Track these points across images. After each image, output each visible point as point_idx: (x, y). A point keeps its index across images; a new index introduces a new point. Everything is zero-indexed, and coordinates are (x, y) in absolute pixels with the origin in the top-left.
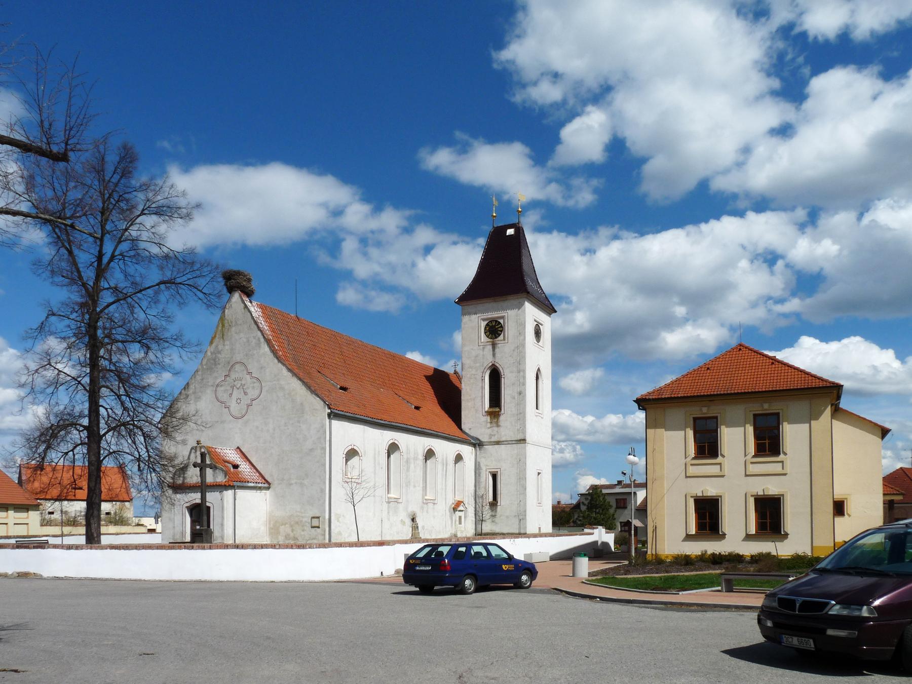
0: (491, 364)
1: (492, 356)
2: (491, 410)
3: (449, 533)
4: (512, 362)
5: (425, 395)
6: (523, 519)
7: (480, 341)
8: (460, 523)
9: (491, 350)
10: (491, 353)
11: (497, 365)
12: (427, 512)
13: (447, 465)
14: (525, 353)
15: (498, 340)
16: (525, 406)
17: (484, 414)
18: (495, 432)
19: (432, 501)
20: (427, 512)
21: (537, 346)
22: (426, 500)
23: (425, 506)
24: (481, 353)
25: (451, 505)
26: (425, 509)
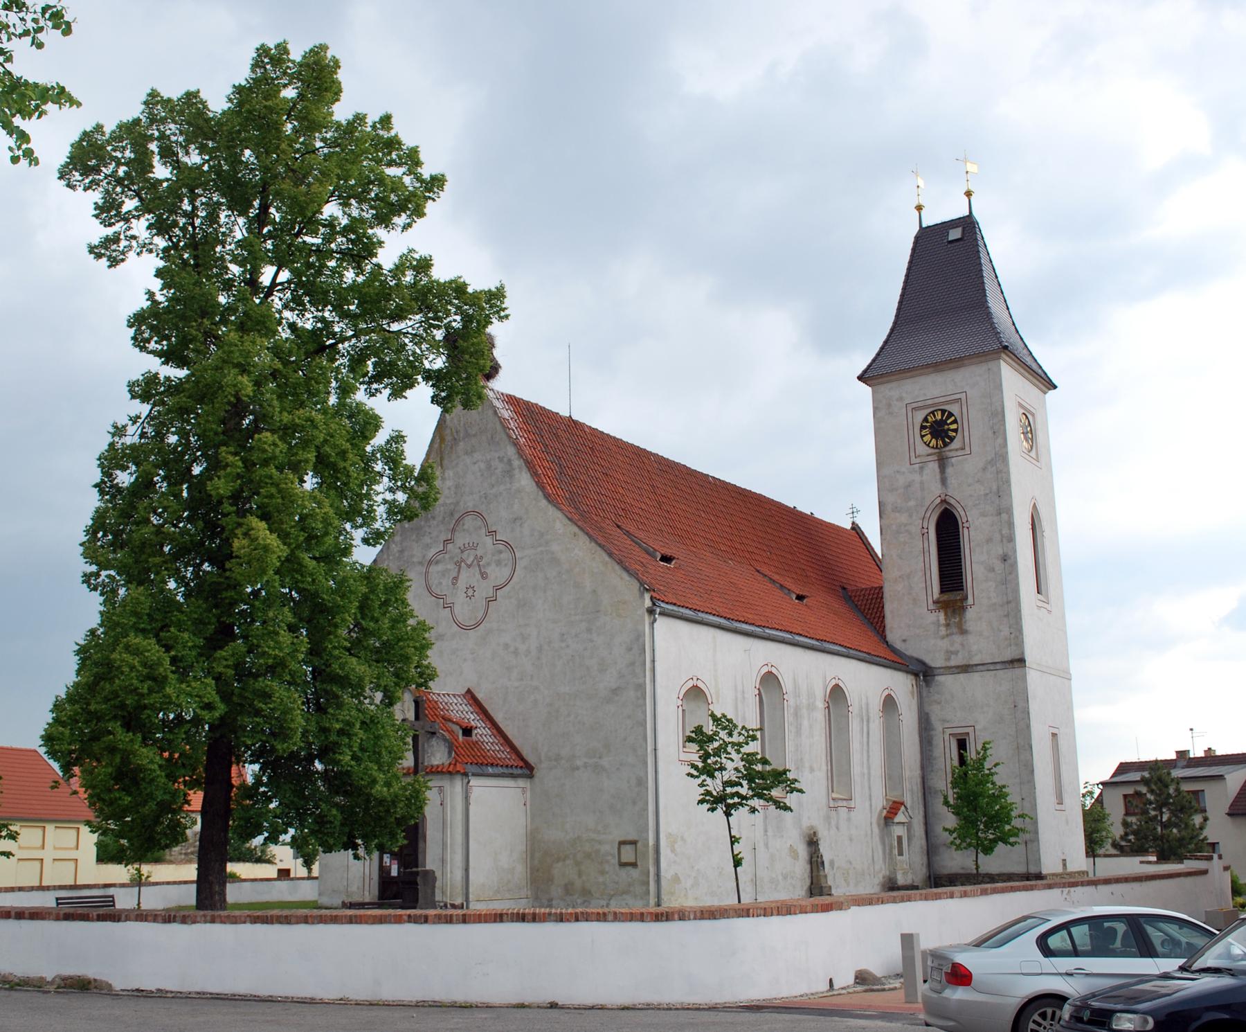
0: (938, 500)
1: (939, 485)
2: (946, 597)
3: (881, 876)
4: (982, 493)
5: (809, 574)
6: (1031, 841)
7: (912, 454)
8: (901, 853)
9: (937, 470)
10: (938, 477)
11: (952, 501)
12: (838, 828)
13: (868, 721)
14: (1008, 473)
15: (950, 451)
16: (1017, 584)
17: (932, 607)
18: (957, 647)
19: (845, 803)
20: (838, 828)
21: (1028, 457)
22: (833, 799)
23: (834, 813)
24: (917, 478)
25: (881, 812)
26: (833, 823)
